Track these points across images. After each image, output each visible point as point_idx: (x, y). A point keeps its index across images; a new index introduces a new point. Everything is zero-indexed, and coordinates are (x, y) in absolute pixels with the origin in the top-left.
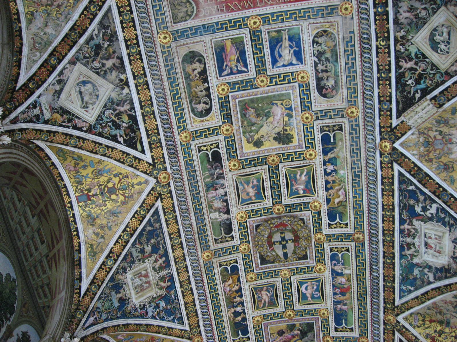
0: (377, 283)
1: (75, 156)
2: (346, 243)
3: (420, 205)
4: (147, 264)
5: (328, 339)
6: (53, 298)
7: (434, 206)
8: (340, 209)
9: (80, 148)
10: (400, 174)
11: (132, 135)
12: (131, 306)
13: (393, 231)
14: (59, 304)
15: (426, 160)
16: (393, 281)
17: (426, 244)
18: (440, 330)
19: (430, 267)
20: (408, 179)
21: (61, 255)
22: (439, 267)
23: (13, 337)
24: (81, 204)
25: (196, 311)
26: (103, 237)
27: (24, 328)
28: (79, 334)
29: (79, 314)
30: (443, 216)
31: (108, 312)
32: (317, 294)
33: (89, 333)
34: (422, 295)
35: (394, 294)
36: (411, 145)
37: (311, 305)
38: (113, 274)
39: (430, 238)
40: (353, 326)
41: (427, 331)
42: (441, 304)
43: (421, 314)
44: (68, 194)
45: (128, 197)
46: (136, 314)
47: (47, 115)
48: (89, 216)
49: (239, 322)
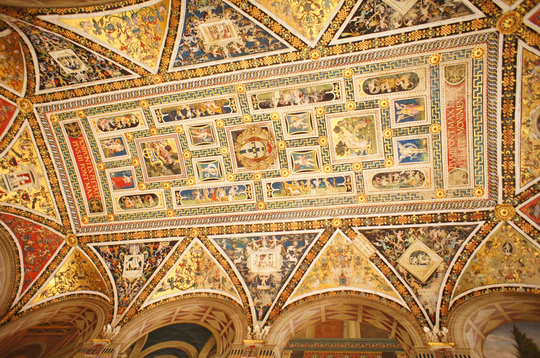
2: (255, 197)
3: (294, 250)
7: (296, 260)
8: (283, 191)
10: (316, 234)
13: (270, 231)
15: (328, 251)
16: (228, 233)
17: (264, 256)
19: (246, 259)
20: (313, 239)
22: (247, 266)
30: (289, 266)
34: (221, 255)
36: (339, 240)
39: (270, 258)
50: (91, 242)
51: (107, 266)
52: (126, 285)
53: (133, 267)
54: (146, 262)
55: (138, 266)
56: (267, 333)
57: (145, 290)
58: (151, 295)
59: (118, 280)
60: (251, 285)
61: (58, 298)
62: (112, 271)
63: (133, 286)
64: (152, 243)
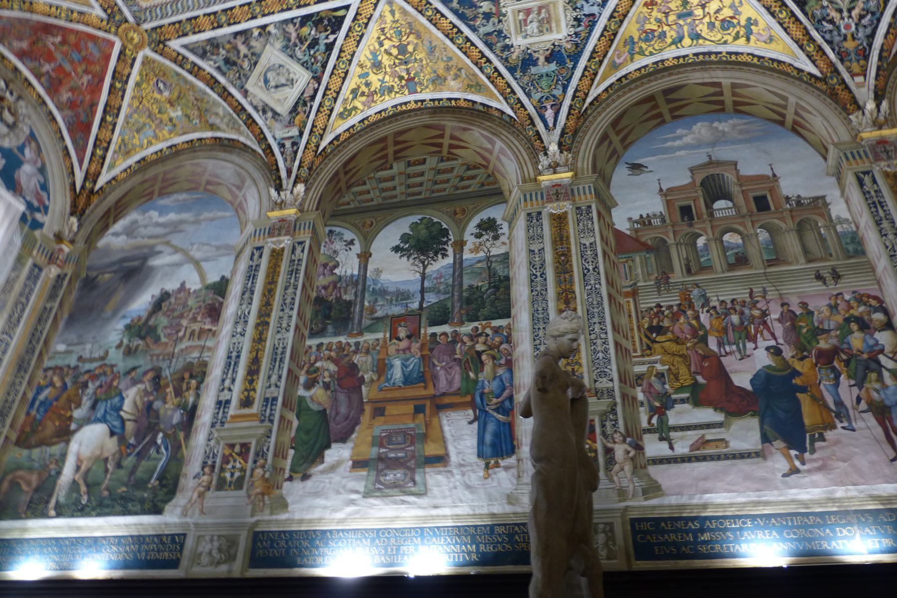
1: (351, 97)
4: (509, 9)
6: (486, 167)
9: (338, 93)
11: (326, 22)
14: (502, 157)
21: (458, 134)
24: (419, 90)
26: (460, 70)
27: (476, 221)
31: (557, 83)
38: (506, 67)
44: (405, 104)
45: (411, 29)
46: (583, 35)
47: (294, 132)
48: (433, 81)
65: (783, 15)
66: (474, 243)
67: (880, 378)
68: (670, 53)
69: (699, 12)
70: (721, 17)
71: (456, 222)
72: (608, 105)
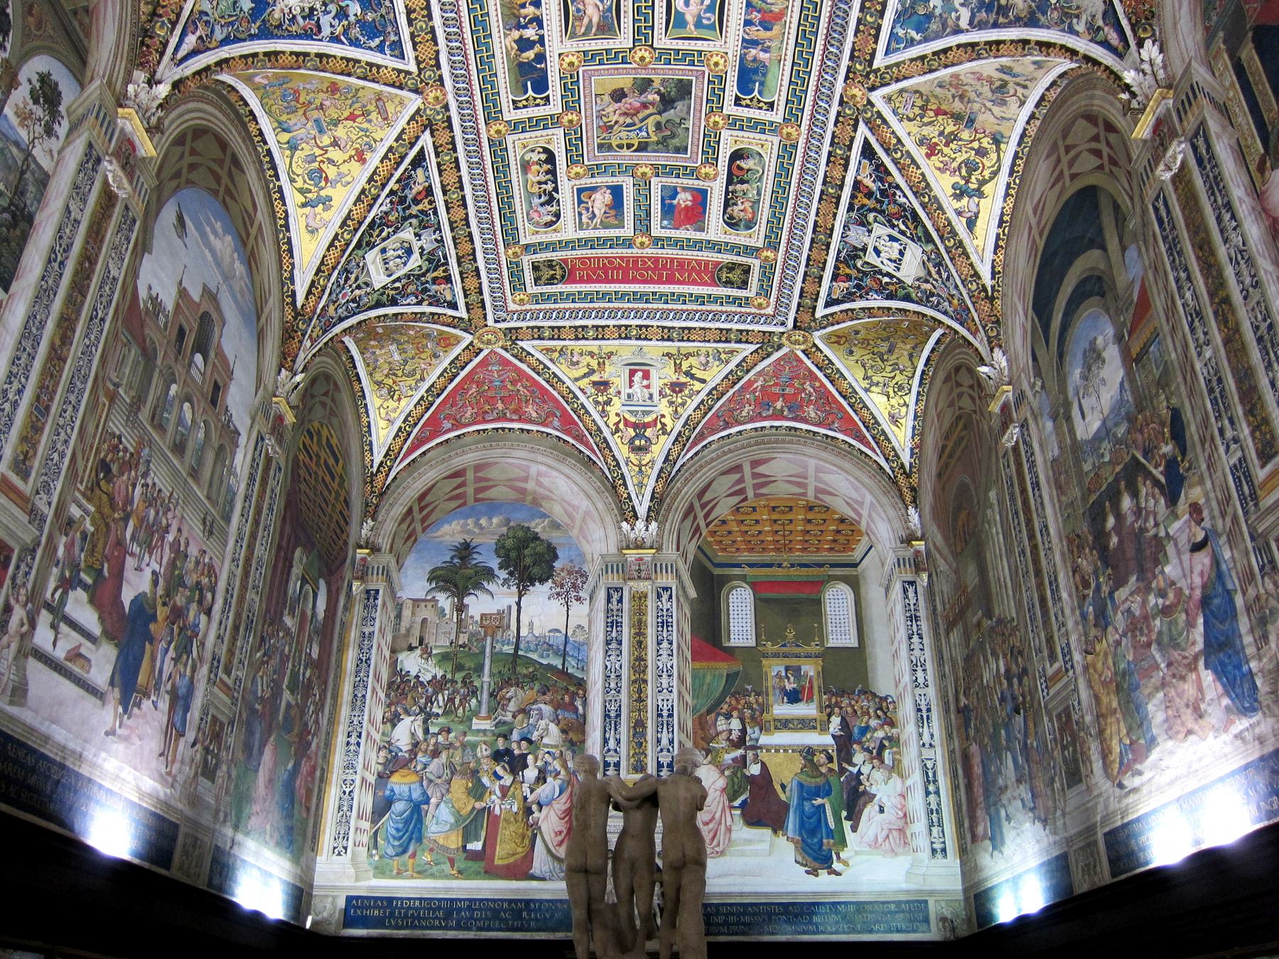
0: (845, 12)
5: (717, 119)
12: (282, 11)
18: (952, 133)
23: (20, 88)
25: (433, 31)
28: (167, 74)
29: (162, 27)
32: (709, 19)
33: (188, 72)
34: (934, 54)
35: (876, 42)
37: (693, 42)
40: (776, 98)
41: (926, 131)
42: (970, 79)
43: (921, 95)
46: (294, 28)
49: (529, 64)
50: (814, 308)
51: (876, 302)
52: (928, 286)
53: (895, 255)
54: (893, 226)
55: (896, 245)
56: (1159, 59)
57: (951, 260)
58: (970, 250)
59: (914, 295)
60: (1039, 15)
61: (917, 400)
62: (890, 297)
63: (936, 276)
64: (853, 197)
65: (347, 236)
66: (26, 104)
67: (186, 665)
68: (265, 123)
69: (326, 140)
70: (324, 167)
71: (24, 28)
72: (200, 99)
